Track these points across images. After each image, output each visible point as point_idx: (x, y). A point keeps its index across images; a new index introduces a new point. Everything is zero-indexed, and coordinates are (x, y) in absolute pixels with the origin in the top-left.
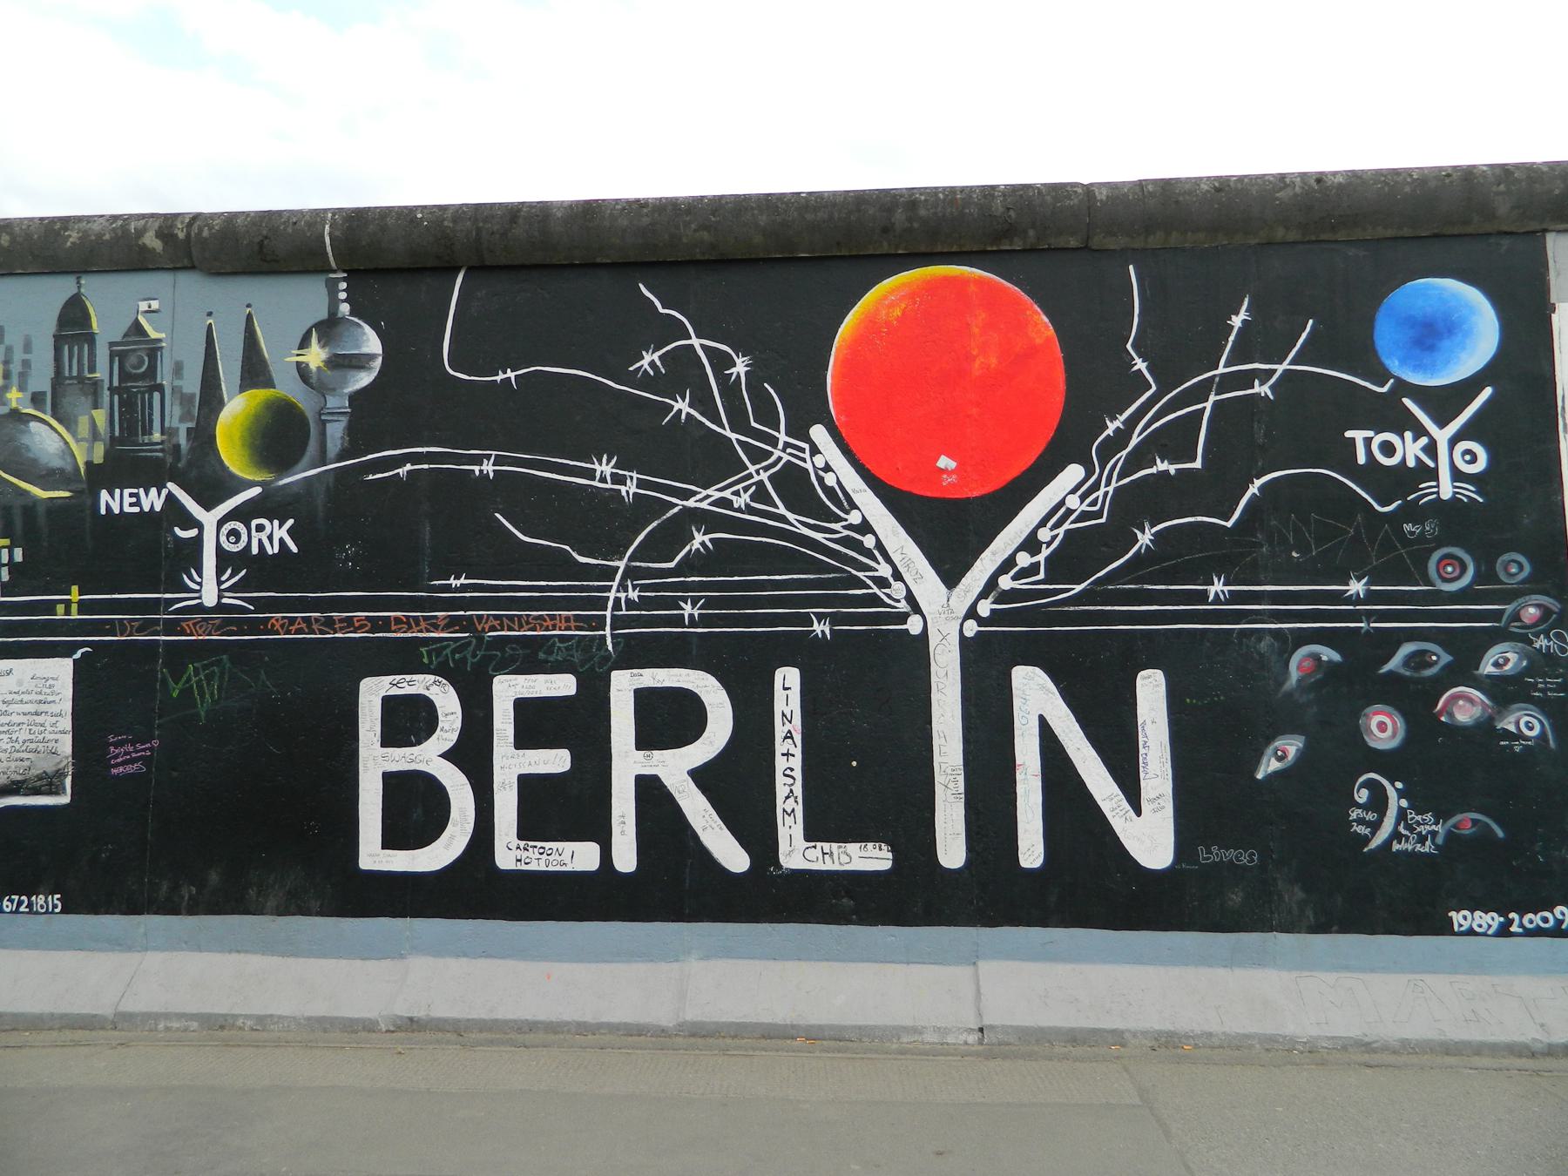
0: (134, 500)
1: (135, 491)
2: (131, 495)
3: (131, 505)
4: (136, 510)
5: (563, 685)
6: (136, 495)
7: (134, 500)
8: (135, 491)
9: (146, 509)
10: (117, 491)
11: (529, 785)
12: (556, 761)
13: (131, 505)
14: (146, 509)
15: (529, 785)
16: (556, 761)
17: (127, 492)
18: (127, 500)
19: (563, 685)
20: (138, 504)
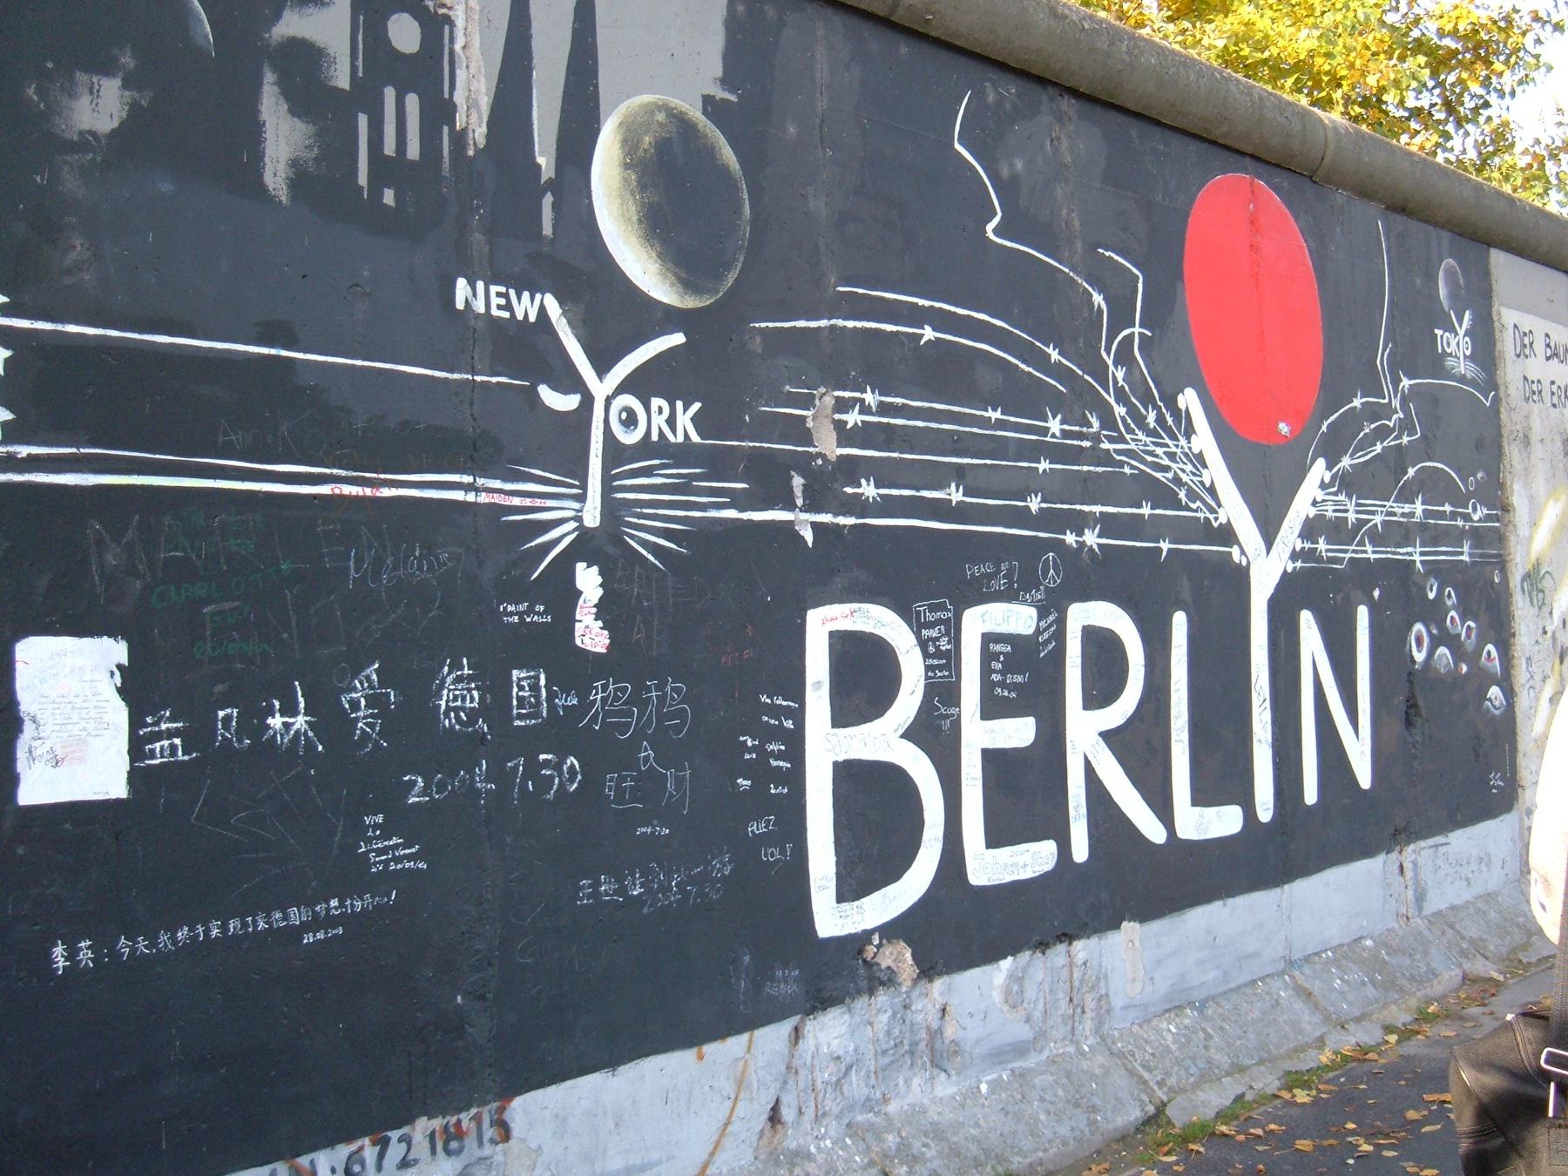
0: (502, 301)
1: (503, 289)
2: (499, 295)
3: (499, 307)
4: (506, 315)
5: (1018, 618)
6: (506, 296)
7: (502, 301)
8: (503, 289)
9: (520, 317)
10: (480, 285)
11: (991, 757)
12: (1018, 732)
13: (499, 307)
14: (520, 317)
15: (991, 757)
16: (1018, 732)
17: (494, 289)
18: (495, 301)
19: (1018, 618)
20: (508, 307)
